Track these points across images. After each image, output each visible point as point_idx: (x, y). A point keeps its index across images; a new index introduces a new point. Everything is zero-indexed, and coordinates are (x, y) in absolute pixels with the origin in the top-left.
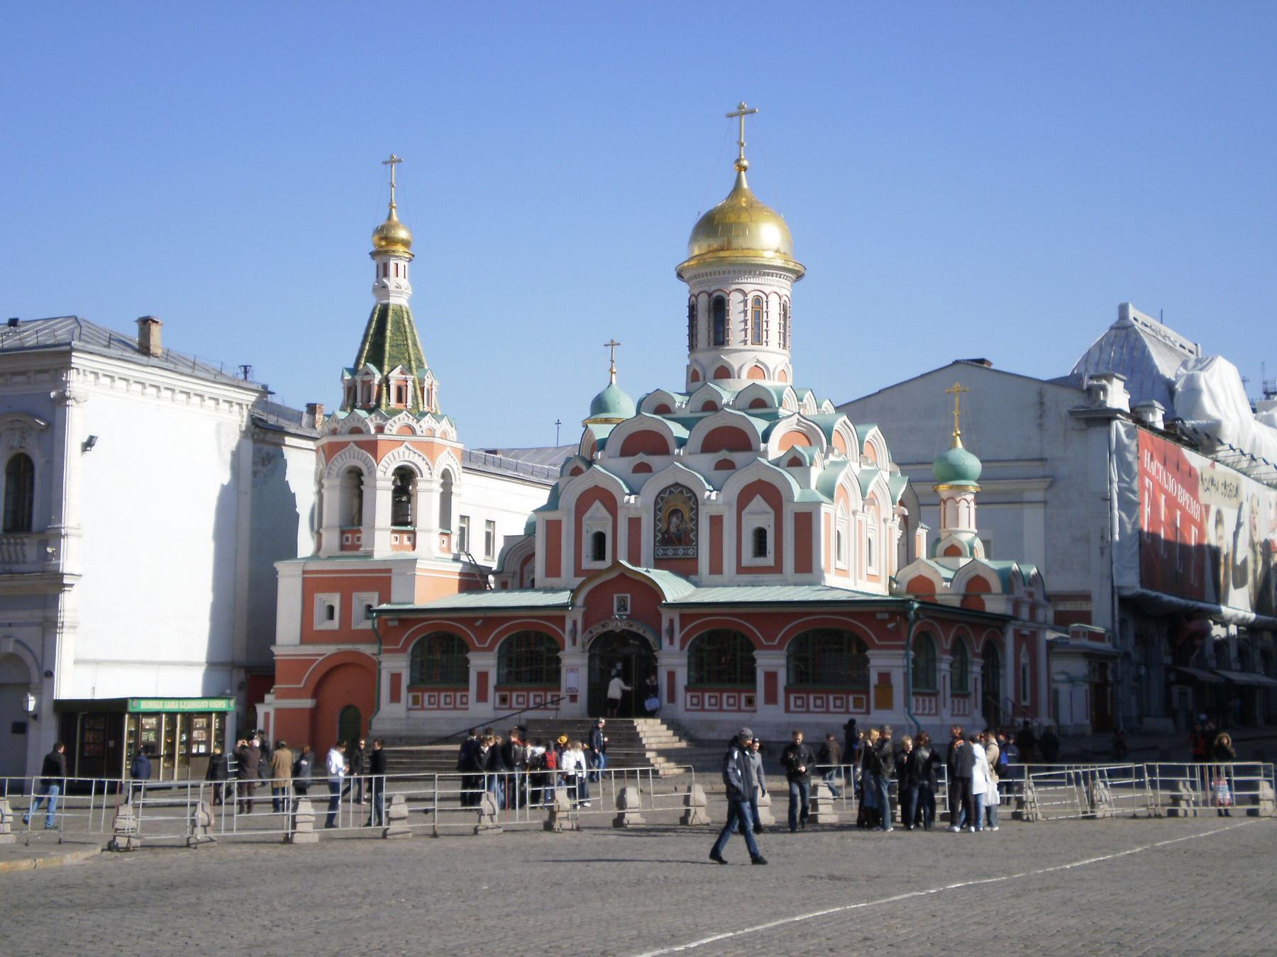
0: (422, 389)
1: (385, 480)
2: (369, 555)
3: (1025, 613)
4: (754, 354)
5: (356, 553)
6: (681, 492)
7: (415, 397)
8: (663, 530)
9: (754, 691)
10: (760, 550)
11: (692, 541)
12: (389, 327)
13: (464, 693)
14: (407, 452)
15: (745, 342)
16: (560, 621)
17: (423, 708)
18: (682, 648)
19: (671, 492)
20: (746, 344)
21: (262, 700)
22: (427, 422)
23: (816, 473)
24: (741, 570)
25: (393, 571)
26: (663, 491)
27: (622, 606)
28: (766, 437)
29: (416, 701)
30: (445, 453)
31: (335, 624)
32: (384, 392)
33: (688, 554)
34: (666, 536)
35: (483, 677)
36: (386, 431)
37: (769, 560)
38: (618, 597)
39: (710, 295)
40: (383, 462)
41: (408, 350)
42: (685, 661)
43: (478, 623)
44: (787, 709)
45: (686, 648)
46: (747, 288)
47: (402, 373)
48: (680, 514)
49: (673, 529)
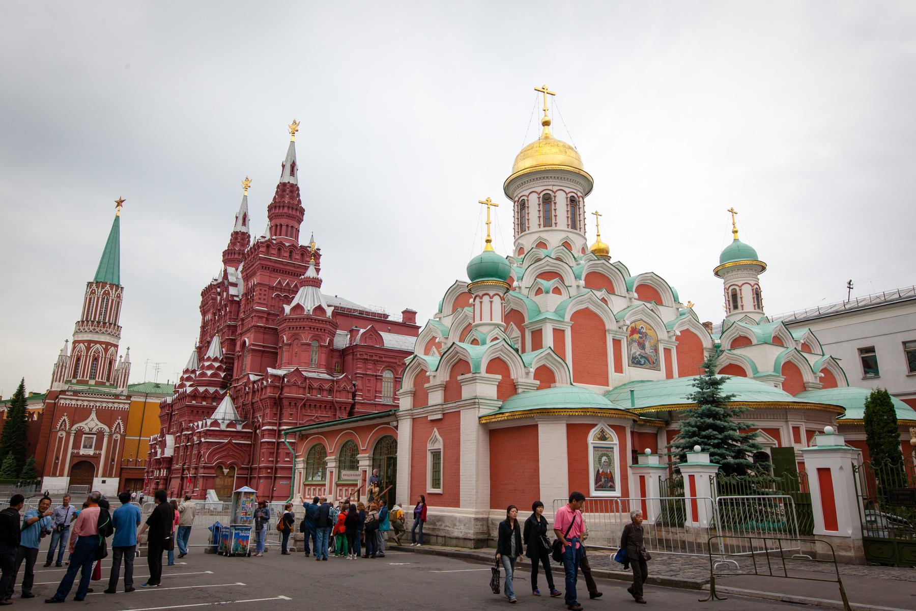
15: (540, 225)
20: (540, 227)
46: (539, 189)
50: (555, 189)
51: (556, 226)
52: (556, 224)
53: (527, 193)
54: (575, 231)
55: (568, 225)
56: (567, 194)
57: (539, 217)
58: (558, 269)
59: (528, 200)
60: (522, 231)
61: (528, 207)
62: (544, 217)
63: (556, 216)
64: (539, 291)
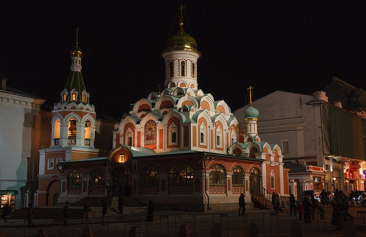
2: (61, 146)
3: (272, 159)
10: (174, 140)
12: (73, 78)
14: (73, 114)
21: (36, 192)
22: (81, 105)
23: (191, 114)
28: (177, 102)
31: (52, 168)
36: (67, 108)
39: (169, 62)
40: (65, 118)
44: (169, 193)
46: (179, 58)
47: (75, 91)
56: (191, 61)
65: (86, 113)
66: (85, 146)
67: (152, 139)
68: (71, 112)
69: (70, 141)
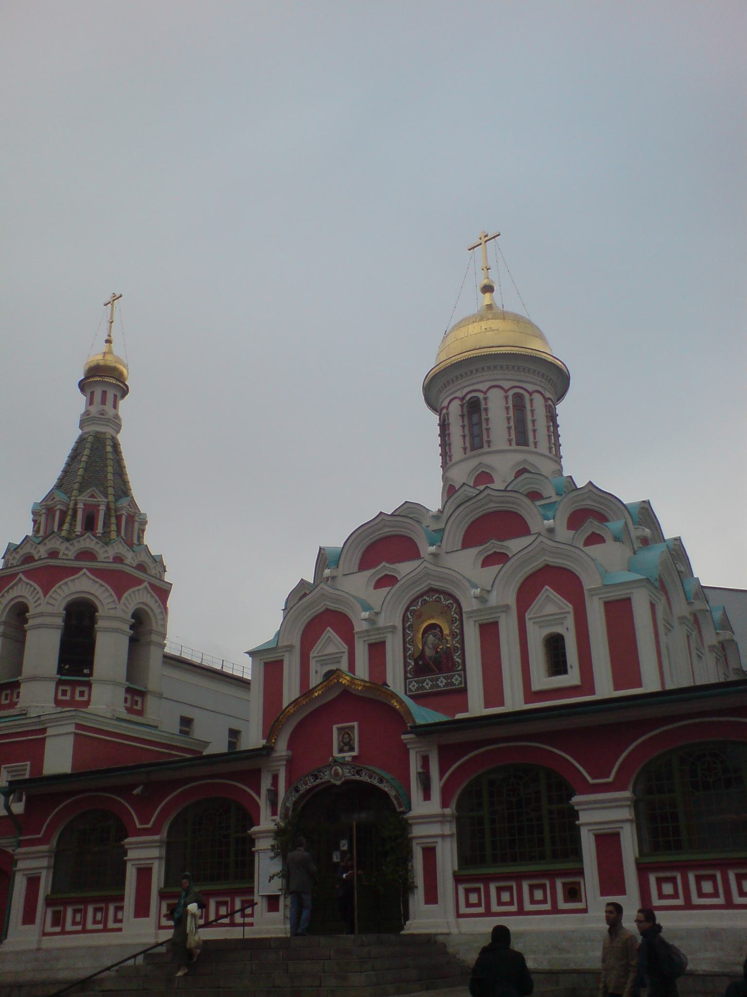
0: (119, 518)
1: (52, 615)
2: (24, 714)
4: (519, 457)
5: (11, 712)
6: (438, 601)
7: (106, 524)
8: (416, 655)
9: (581, 872)
11: (454, 664)
13: (118, 904)
16: (253, 778)
17: (63, 932)
18: (445, 804)
19: (425, 602)
24: (530, 695)
25: (49, 732)
26: (413, 602)
27: (345, 744)
29: (58, 920)
30: (141, 587)
32: (68, 519)
33: (452, 684)
34: (420, 663)
35: (144, 873)
36: (60, 556)
37: (572, 678)
38: (339, 729)
40: (50, 593)
41: (106, 476)
42: (449, 829)
43: (137, 791)
45: (454, 804)
46: (506, 385)
47: (92, 496)
48: (438, 629)
49: (429, 652)
50: (531, 388)
51: (536, 448)
52: (535, 444)
53: (483, 387)
54: (556, 458)
55: (550, 448)
56: (546, 399)
57: (509, 428)
58: (602, 507)
59: (486, 399)
60: (473, 448)
61: (486, 410)
62: (515, 429)
63: (534, 431)
64: (595, 539)
65: (140, 582)
66: (125, 715)
67: (441, 671)
68: (75, 570)
69: (64, 693)
